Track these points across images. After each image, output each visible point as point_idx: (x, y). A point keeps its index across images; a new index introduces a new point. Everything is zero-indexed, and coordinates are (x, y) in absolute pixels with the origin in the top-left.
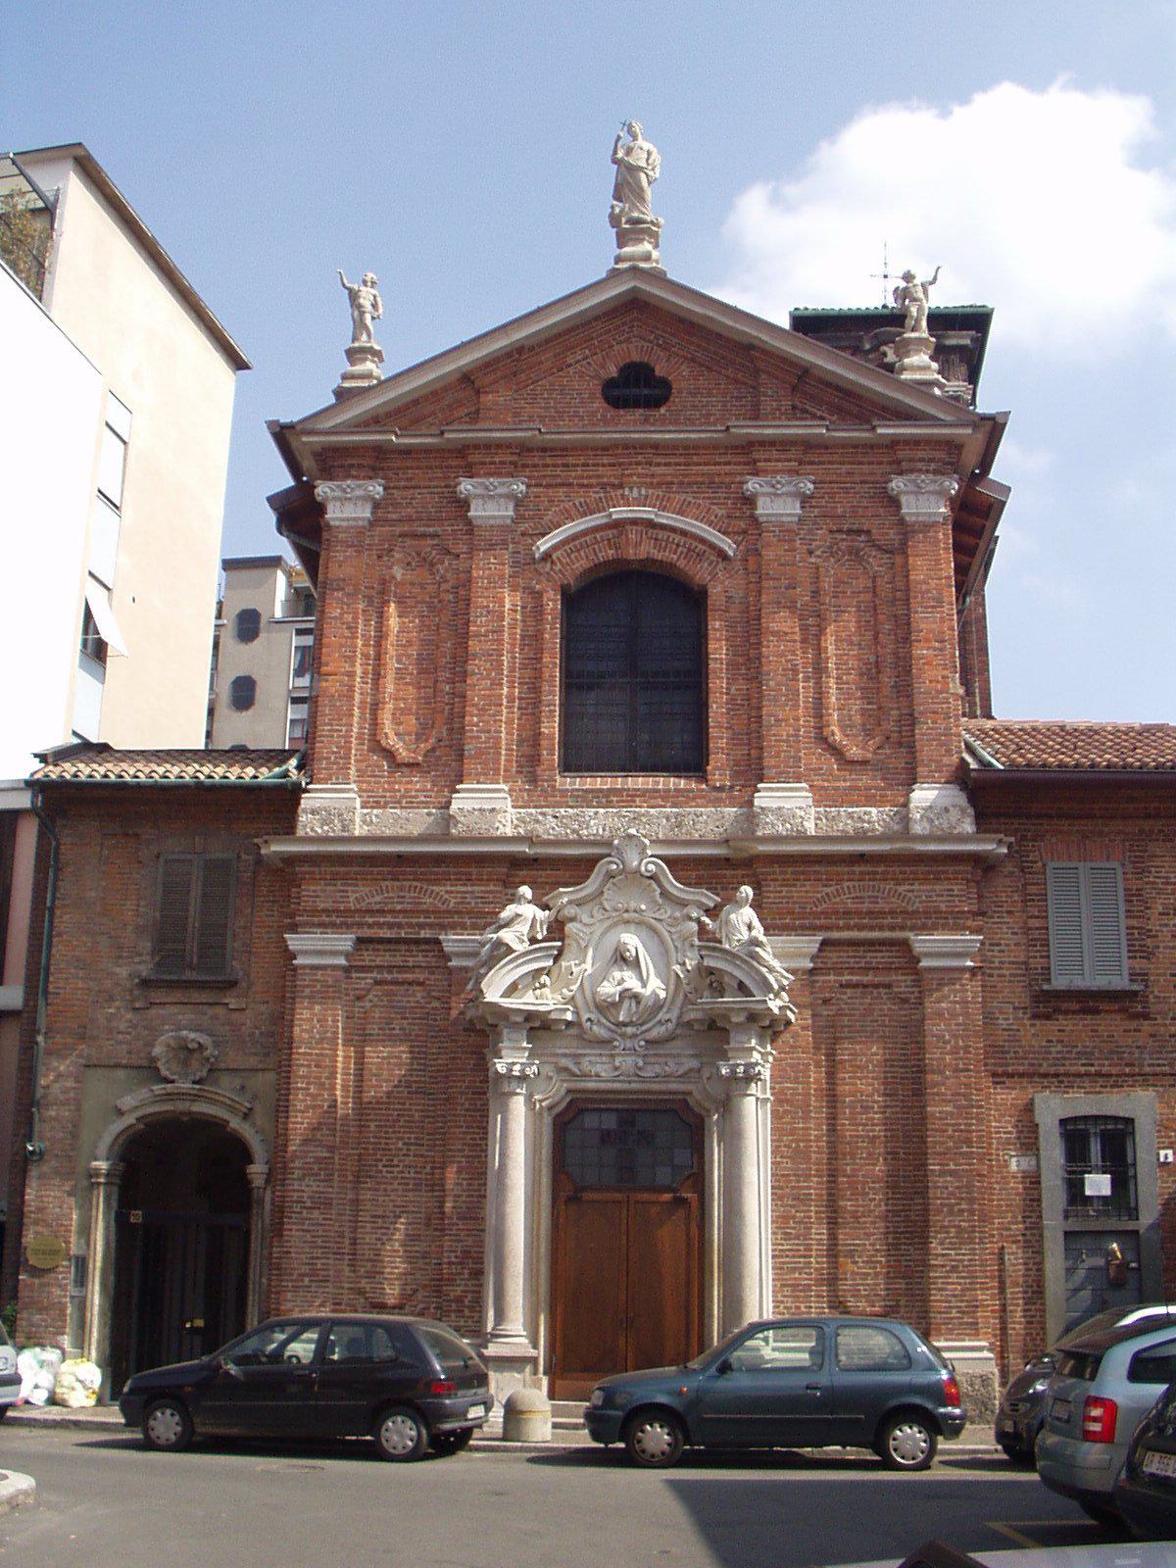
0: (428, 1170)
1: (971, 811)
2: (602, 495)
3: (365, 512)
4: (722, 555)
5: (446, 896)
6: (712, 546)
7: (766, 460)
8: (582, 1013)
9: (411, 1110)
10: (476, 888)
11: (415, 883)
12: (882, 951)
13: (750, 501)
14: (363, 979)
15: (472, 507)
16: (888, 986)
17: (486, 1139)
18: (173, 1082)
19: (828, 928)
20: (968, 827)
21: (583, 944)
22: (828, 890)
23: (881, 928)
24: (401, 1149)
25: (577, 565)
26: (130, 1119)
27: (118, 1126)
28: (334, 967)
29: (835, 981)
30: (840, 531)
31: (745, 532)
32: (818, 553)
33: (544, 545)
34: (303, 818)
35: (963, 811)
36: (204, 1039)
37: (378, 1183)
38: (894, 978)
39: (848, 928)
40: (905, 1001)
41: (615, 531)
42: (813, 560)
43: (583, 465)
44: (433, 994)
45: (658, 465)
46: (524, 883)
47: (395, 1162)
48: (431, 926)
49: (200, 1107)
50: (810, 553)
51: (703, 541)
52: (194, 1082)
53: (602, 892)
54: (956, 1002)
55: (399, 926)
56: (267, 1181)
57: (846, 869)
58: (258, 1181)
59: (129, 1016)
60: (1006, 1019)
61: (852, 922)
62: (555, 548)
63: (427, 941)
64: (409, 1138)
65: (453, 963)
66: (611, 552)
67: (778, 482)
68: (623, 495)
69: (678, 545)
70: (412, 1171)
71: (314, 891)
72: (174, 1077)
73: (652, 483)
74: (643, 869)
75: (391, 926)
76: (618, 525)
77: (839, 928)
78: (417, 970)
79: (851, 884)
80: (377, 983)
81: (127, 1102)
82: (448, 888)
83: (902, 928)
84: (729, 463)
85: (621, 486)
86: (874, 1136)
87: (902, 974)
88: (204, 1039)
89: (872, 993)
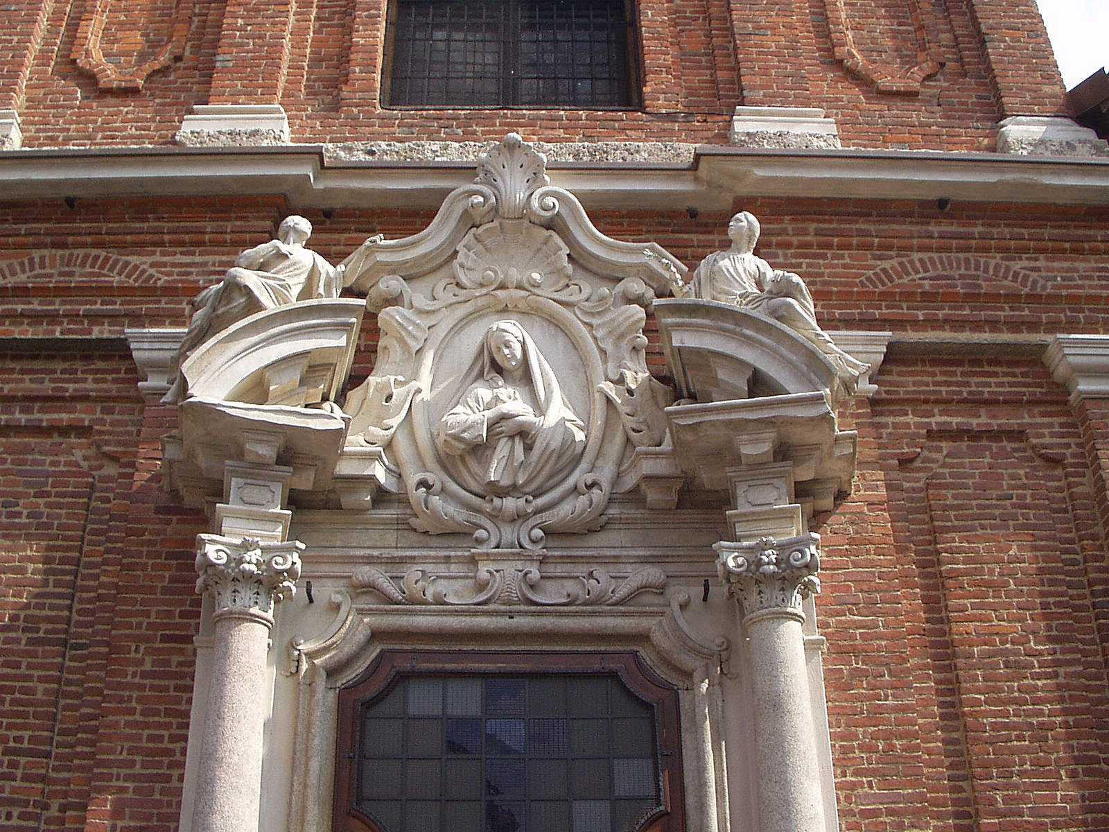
0: (54, 811)
5: (152, 271)
9: (29, 678)
10: (210, 258)
11: (95, 252)
12: (996, 374)
16: (1018, 435)
17: (185, 739)
21: (415, 346)
22: (886, 264)
23: (994, 325)
29: (918, 425)
38: (1027, 420)
39: (933, 323)
40: (1054, 462)
44: (106, 448)
48: (114, 317)
55: (53, 318)
57: (915, 228)
61: (941, 314)
64: (18, 739)
74: (535, 203)
77: (915, 324)
79: (925, 256)
82: (157, 258)
83: (1033, 326)
86: (1042, 726)
87: (1043, 415)
89: (990, 448)
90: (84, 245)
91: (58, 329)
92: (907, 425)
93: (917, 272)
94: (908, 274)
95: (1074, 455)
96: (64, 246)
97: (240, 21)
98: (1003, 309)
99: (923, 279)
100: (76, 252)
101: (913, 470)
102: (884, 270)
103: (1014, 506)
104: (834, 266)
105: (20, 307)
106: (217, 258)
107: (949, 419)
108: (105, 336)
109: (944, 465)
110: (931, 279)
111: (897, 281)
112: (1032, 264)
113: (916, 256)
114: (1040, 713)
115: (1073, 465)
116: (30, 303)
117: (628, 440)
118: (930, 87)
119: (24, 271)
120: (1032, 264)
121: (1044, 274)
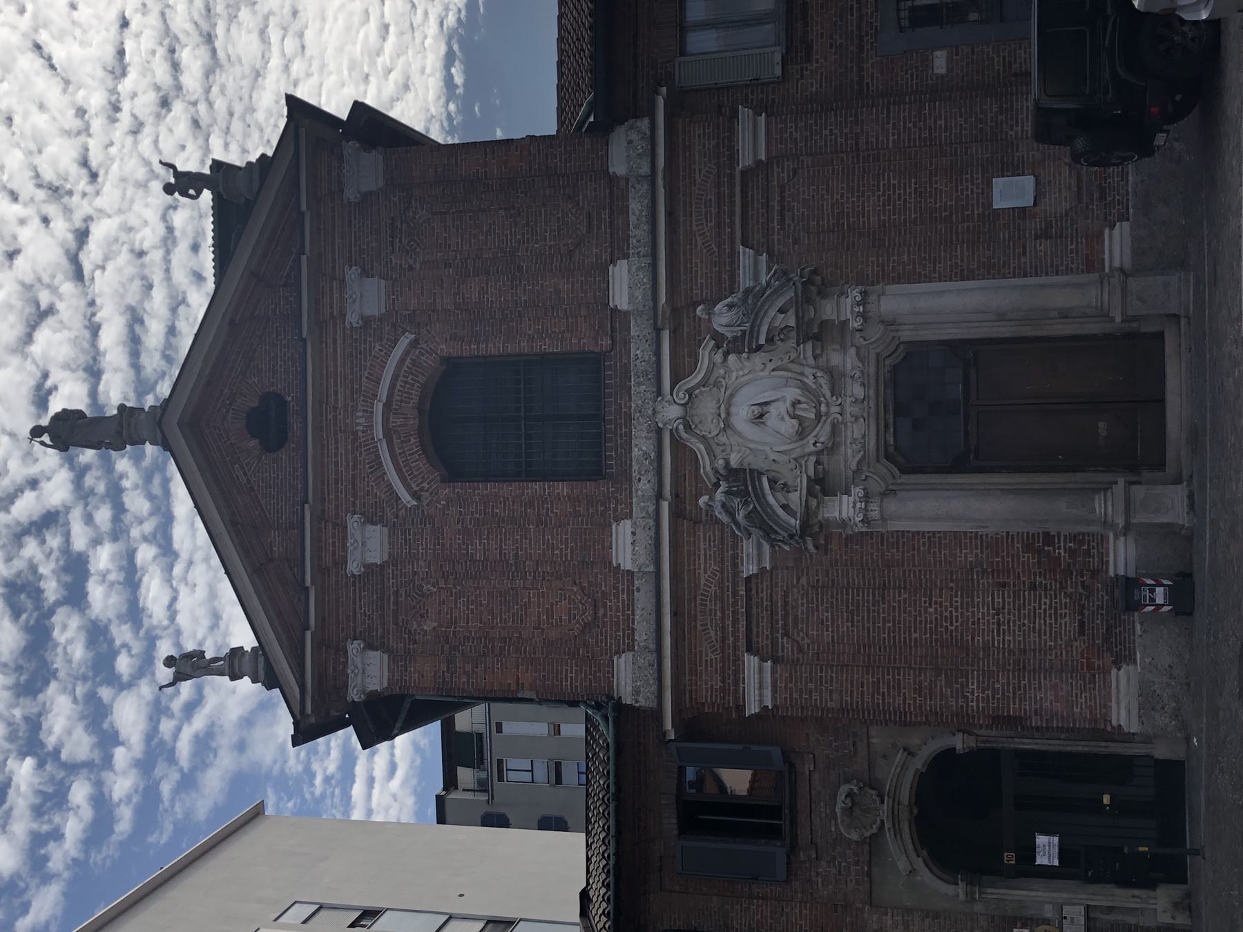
1: (631, 121)
3: (374, 657)
4: (414, 344)
5: (709, 572)
6: (407, 353)
7: (332, 307)
9: (899, 601)
11: (698, 601)
12: (752, 196)
13: (367, 321)
14: (783, 646)
15: (372, 561)
16: (782, 188)
18: (882, 821)
20: (644, 124)
21: (748, 451)
23: (732, 195)
24: (936, 609)
25: (423, 468)
26: (919, 863)
27: (925, 875)
29: (779, 234)
30: (392, 244)
31: (394, 326)
32: (412, 263)
34: (642, 702)
35: (631, 128)
36: (844, 789)
37: (967, 630)
38: (776, 183)
39: (732, 225)
40: (795, 172)
41: (394, 437)
42: (418, 266)
44: (795, 583)
45: (336, 400)
46: (697, 504)
47: (948, 614)
48: (735, 584)
49: (905, 796)
50: (411, 268)
51: (402, 361)
52: (882, 802)
53: (703, 436)
54: (796, 127)
55: (735, 613)
56: (970, 734)
57: (681, 228)
58: (972, 743)
59: (824, 863)
60: (812, 86)
61: (727, 221)
62: (408, 488)
63: (748, 590)
64: (925, 602)
65: (767, 565)
66: (413, 440)
69: (406, 383)
70: (955, 599)
72: (878, 821)
73: (352, 406)
74: (683, 402)
75: (736, 621)
76: (387, 434)
77: (733, 233)
78: (774, 598)
79: (694, 223)
80: (786, 634)
81: (902, 865)
82: (702, 571)
83: (732, 177)
84: (335, 341)
85: (355, 433)
86: (915, 193)
87: (773, 176)
88: (844, 789)
89: (789, 202)
90: (695, 606)
91: (740, 610)
92: (779, 239)
93: (704, 228)
94: (705, 233)
95: (793, 164)
96: (696, 615)
97: (556, 552)
98: (724, 191)
99: (707, 226)
100: (698, 609)
101: (800, 238)
102: (703, 244)
103: (818, 194)
104: (701, 267)
105: (731, 629)
106: (702, 543)
107: (776, 220)
108: (744, 588)
109: (798, 224)
110: (707, 222)
111: (709, 238)
112: (697, 172)
113: (694, 228)
114: (910, 193)
115: (798, 164)
116: (728, 625)
117: (792, 361)
118: (583, 205)
119: (709, 633)
120: (697, 172)
121: (703, 167)
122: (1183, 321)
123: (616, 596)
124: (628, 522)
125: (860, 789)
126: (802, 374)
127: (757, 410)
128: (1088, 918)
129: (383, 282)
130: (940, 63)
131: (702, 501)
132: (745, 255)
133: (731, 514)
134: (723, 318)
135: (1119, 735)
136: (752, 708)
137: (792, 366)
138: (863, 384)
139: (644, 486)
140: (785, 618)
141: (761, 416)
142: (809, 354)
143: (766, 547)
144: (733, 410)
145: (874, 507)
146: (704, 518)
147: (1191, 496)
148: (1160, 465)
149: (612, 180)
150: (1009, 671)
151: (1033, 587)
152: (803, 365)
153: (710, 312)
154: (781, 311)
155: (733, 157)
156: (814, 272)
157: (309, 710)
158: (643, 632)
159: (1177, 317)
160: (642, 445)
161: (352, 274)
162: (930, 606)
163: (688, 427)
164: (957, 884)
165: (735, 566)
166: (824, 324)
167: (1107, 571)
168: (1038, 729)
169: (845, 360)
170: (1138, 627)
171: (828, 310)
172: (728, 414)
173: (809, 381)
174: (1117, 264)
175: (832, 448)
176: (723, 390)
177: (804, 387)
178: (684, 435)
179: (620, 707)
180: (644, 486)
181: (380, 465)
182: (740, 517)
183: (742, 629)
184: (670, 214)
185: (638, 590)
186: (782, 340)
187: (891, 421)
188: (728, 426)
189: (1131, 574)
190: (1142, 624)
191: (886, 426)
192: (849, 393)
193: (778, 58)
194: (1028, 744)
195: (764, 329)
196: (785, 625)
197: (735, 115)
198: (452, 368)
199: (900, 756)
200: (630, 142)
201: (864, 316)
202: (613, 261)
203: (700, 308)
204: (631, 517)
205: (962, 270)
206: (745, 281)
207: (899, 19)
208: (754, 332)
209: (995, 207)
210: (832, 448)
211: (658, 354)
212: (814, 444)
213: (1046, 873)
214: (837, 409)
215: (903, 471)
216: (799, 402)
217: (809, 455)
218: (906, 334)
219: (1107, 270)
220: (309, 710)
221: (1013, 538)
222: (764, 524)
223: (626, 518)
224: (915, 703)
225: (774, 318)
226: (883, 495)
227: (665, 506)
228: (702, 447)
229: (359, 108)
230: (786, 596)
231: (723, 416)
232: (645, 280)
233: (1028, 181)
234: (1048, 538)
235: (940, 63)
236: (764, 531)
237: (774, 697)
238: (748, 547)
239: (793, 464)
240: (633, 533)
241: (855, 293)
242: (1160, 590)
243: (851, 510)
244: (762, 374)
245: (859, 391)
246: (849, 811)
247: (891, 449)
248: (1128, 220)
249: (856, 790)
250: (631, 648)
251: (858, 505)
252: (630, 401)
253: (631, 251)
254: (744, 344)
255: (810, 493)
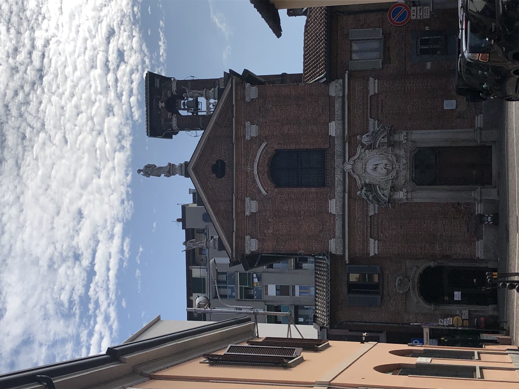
1: (336, 80)
2: (250, 177)
4: (267, 145)
6: (264, 148)
7: (241, 134)
8: (389, 179)
11: (356, 223)
13: (252, 138)
14: (381, 236)
18: (410, 288)
19: (367, 116)
20: (341, 81)
22: (357, 117)
24: (426, 225)
25: (269, 184)
26: (420, 300)
27: (422, 303)
28: (378, 243)
33: (264, 192)
34: (338, 253)
36: (398, 278)
40: (386, 96)
41: (260, 174)
42: (268, 122)
43: (241, 182)
46: (357, 193)
47: (430, 226)
48: (367, 218)
51: (263, 151)
52: (409, 282)
58: (436, 264)
59: (392, 301)
61: (366, 111)
62: (264, 189)
65: (377, 212)
66: (265, 175)
67: (247, 131)
68: (249, 172)
69: (264, 157)
70: (432, 222)
71: (358, 249)
73: (246, 164)
74: (352, 164)
79: (355, 111)
81: (415, 300)
85: (247, 172)
88: (398, 278)
117: (385, 152)
122: (497, 143)
123: (330, 222)
124: (334, 200)
125: (403, 278)
126: (388, 156)
127: (374, 166)
128: (469, 314)
129: (257, 126)
130: (429, 65)
131: (358, 193)
132: (371, 121)
133: (368, 197)
134: (365, 139)
135: (479, 260)
136: (372, 254)
137: (385, 154)
138: (406, 159)
139: (339, 189)
140: (381, 228)
141: (375, 168)
142: (390, 150)
143: (377, 206)
144: (367, 166)
145: (409, 195)
146: (357, 199)
147: (498, 192)
148: (490, 183)
149: (330, 97)
150: (447, 242)
151: (454, 218)
152: (388, 153)
153: (361, 137)
154: (383, 138)
155: (368, 92)
156: (391, 126)
157: (234, 256)
158: (338, 232)
159: (495, 142)
160: (338, 177)
161: (248, 124)
162: (424, 224)
163: (353, 171)
164: (431, 305)
165: (367, 212)
166: (395, 142)
167: (475, 214)
168: (456, 259)
169: (402, 153)
170: (484, 229)
171: (396, 138)
172: (365, 168)
173: (390, 158)
174: (479, 126)
175: (396, 178)
176: (364, 161)
177: (389, 160)
178: (352, 174)
179: (331, 254)
180: (339, 189)
181: (255, 182)
182: (370, 197)
183: (369, 231)
184: (348, 108)
185: (337, 220)
186: (382, 146)
187: (414, 171)
188: (365, 171)
189: (482, 213)
190: (484, 228)
191: (413, 172)
192: (401, 161)
193: (381, 62)
194: (452, 264)
195: (378, 143)
196: (381, 230)
197: (368, 80)
198: (278, 152)
199: (415, 268)
200: (336, 87)
201: (407, 140)
202: (330, 121)
203: (359, 136)
204: (335, 198)
205: (435, 127)
206: (371, 130)
207: (417, 52)
208: (375, 143)
209: (445, 109)
210: (396, 178)
211: (344, 149)
212: (391, 177)
213: (458, 302)
214: (398, 166)
215: (417, 185)
216: (387, 164)
217: (390, 180)
218: (419, 145)
219: (476, 128)
220: (234, 256)
221: (449, 204)
222: (377, 199)
223: (333, 199)
224: (420, 252)
225: (381, 139)
226: (412, 191)
227: (347, 195)
228: (357, 177)
229: (246, 71)
230: (382, 222)
231: (364, 168)
232: (340, 127)
233: (454, 102)
234: (459, 204)
235: (429, 65)
236: (377, 202)
237: (378, 251)
238: (371, 207)
239: (385, 182)
240: (336, 203)
241: (405, 133)
242: (489, 218)
243: (403, 196)
244: (376, 156)
245: (404, 161)
246: (399, 285)
247: (414, 178)
248: (482, 114)
249: (402, 278)
250: (334, 237)
251: (405, 194)
252: (335, 163)
253: (336, 119)
254: (371, 147)
255: (391, 190)
